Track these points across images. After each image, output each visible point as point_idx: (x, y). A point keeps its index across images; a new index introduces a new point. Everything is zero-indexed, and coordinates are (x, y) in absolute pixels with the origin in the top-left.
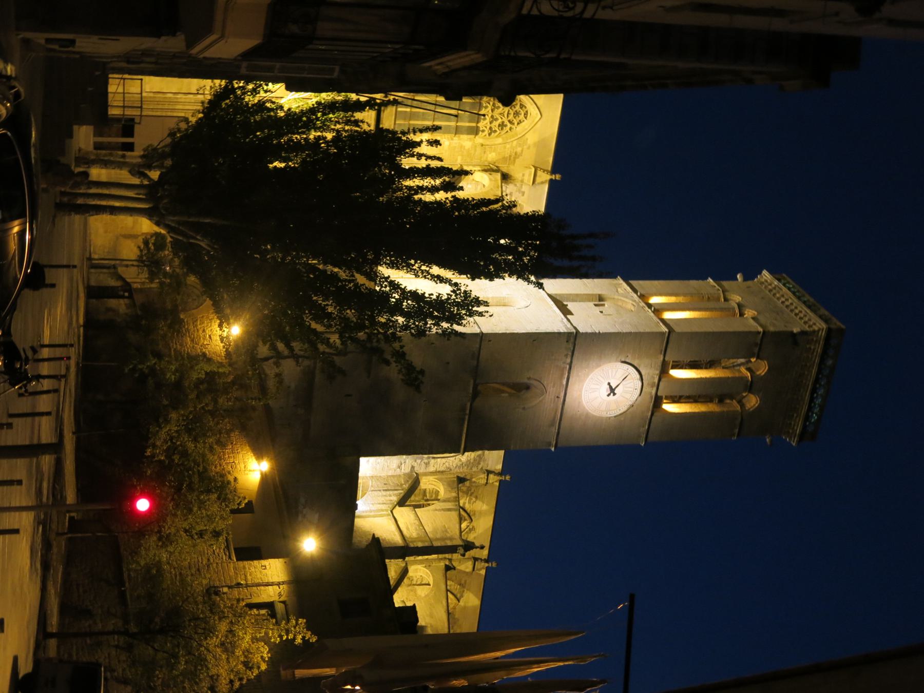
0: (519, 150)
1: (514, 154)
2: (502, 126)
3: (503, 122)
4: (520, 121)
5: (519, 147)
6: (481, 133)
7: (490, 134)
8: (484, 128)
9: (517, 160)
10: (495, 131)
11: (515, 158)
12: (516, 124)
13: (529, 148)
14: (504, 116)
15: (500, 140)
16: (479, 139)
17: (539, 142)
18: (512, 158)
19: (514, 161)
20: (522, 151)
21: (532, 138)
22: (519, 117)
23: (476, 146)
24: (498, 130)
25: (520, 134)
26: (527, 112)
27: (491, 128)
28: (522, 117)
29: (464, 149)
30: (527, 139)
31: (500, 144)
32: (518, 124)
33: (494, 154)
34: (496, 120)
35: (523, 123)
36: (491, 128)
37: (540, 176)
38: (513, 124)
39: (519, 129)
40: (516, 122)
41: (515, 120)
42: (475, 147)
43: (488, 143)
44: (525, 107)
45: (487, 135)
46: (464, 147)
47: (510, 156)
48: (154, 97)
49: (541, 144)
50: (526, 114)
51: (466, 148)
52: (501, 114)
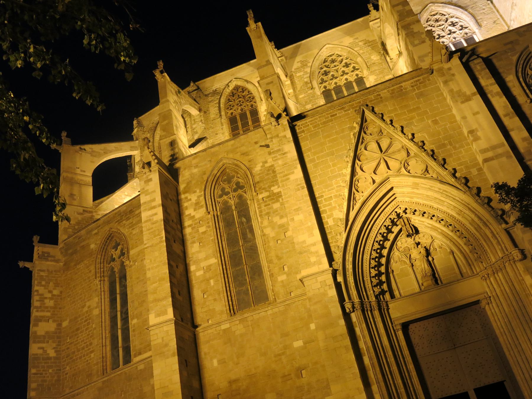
0: (360, 43)
1: (366, 45)
2: (347, 65)
3: (344, 66)
4: (338, 57)
5: (358, 44)
6: (359, 76)
7: (358, 69)
8: (354, 75)
9: (370, 40)
10: (354, 67)
11: (369, 42)
12: (341, 58)
13: (357, 38)
14: (338, 69)
15: (359, 59)
16: (365, 73)
17: (348, 35)
18: (370, 44)
19: (372, 41)
20: (361, 41)
21: (348, 41)
22: (335, 59)
23: (372, 72)
24: (352, 66)
25: (348, 50)
26: (328, 56)
27: (352, 71)
28: (333, 57)
29: (378, 78)
30: (350, 43)
31: (362, 57)
32: (341, 56)
33: (372, 57)
34: (343, 72)
35: (339, 53)
36: (352, 71)
37: (375, 16)
38: (342, 60)
39: (345, 54)
40: (340, 58)
41: (339, 60)
42: (372, 73)
43: (365, 65)
44: (325, 59)
45: (359, 71)
46: (375, 79)
47: (369, 46)
48: (378, 382)
49: (349, 33)
50: (331, 56)
51: (376, 77)
52: (337, 71)
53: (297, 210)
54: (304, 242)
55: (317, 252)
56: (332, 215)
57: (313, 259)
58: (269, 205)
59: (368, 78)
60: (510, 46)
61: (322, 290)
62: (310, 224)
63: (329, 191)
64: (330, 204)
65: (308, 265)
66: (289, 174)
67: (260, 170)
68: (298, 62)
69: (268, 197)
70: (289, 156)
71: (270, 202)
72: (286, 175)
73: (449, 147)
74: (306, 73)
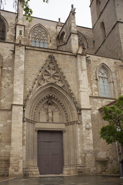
30: (48, 28)
53: (18, 80)
54: (17, 92)
55: (20, 97)
56: (29, 87)
57: (18, 99)
58: (5, 73)
59: (49, 44)
60: (98, 60)
61: (18, 111)
62: (21, 87)
63: (31, 78)
64: (29, 83)
65: (16, 100)
66: (19, 66)
67: (6, 59)
68: (27, 24)
69: (6, 70)
70: (21, 59)
71: (6, 72)
72: (18, 66)
73: (72, 82)
74: (29, 29)
